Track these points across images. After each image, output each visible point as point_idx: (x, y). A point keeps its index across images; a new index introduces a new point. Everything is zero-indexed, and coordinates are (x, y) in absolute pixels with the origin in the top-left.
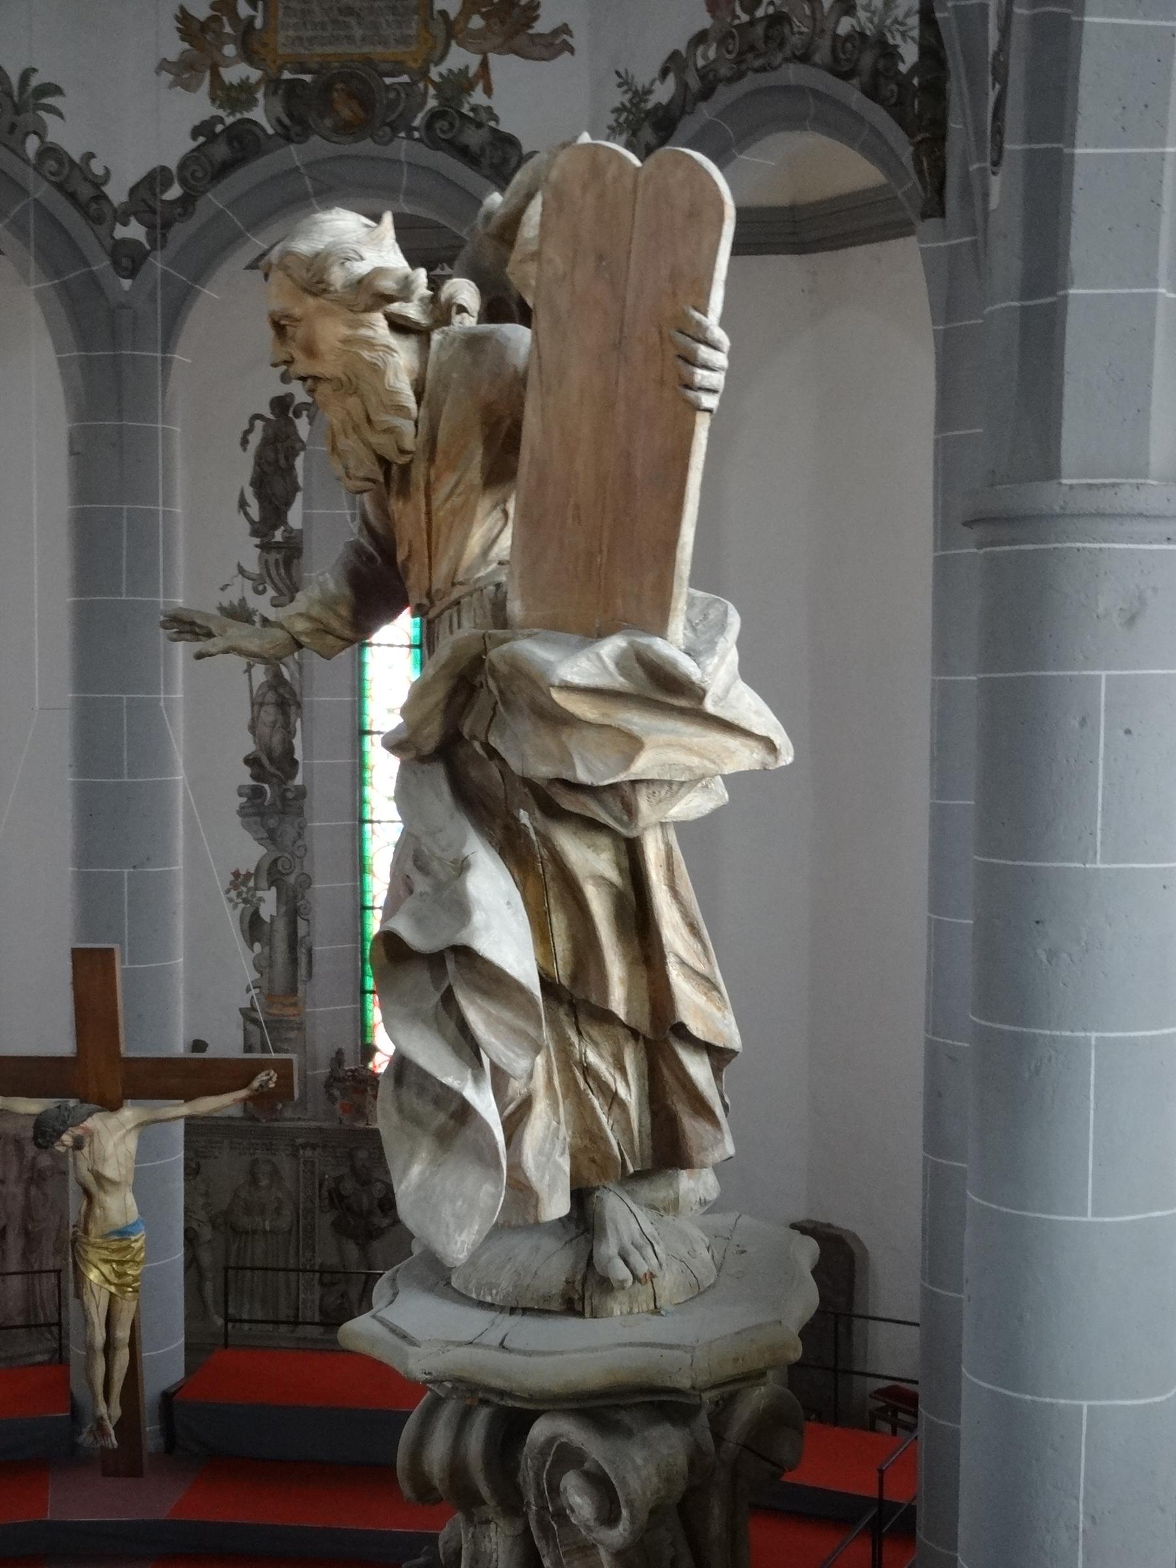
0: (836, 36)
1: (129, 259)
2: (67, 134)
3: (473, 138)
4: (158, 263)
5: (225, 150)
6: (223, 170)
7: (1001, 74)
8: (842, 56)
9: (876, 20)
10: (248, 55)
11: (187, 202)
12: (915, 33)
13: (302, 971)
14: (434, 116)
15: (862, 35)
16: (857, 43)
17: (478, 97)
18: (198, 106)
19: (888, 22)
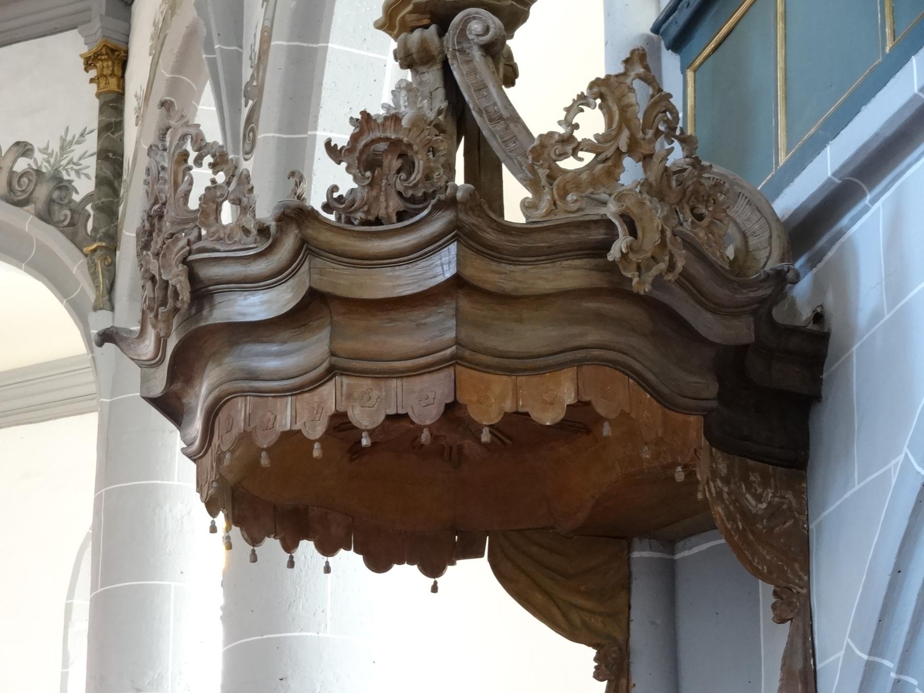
0: (12, 173)
7: (255, 92)
8: (17, 187)
9: (52, 160)
12: (92, 172)
15: (38, 172)
16: (34, 178)
19: (64, 162)
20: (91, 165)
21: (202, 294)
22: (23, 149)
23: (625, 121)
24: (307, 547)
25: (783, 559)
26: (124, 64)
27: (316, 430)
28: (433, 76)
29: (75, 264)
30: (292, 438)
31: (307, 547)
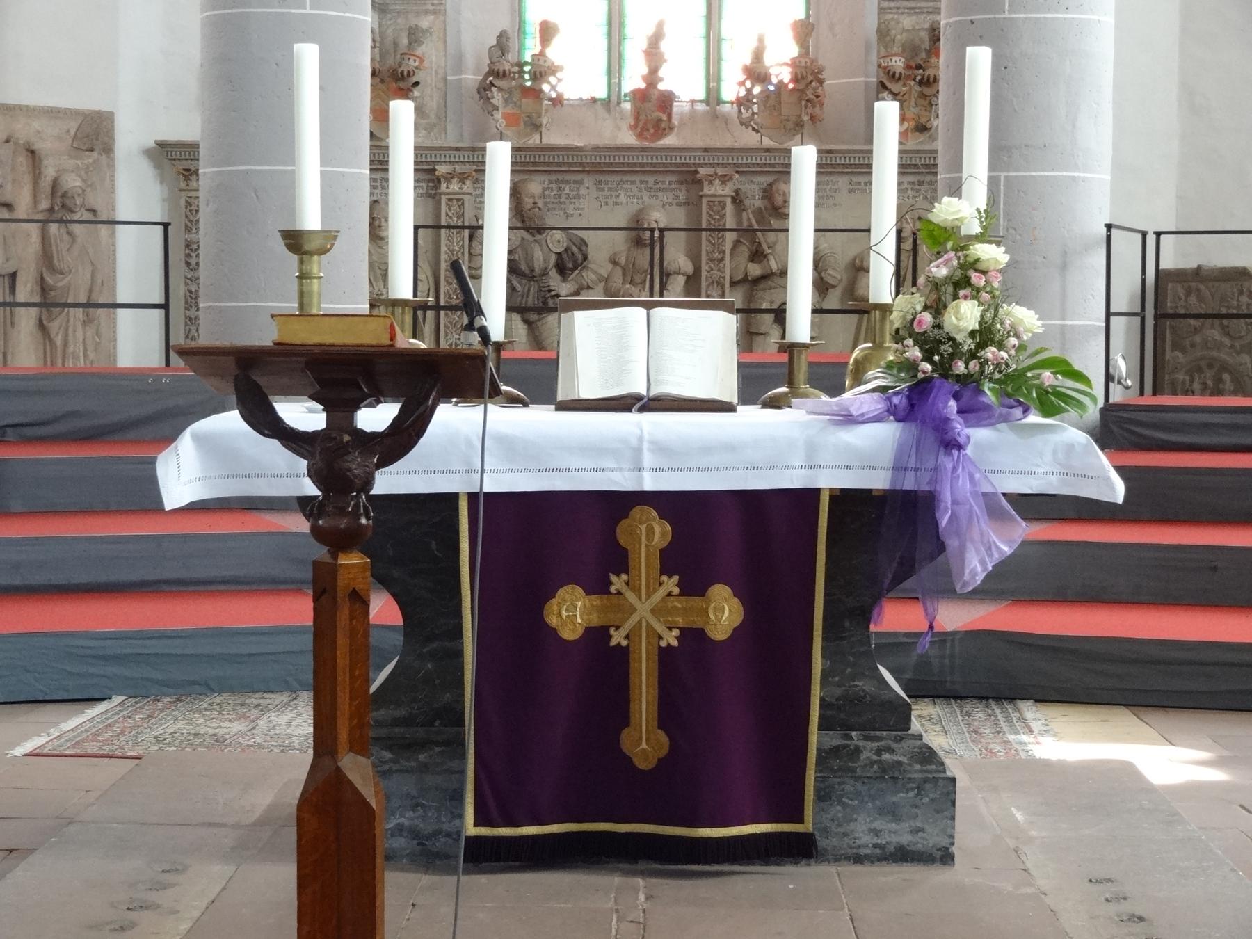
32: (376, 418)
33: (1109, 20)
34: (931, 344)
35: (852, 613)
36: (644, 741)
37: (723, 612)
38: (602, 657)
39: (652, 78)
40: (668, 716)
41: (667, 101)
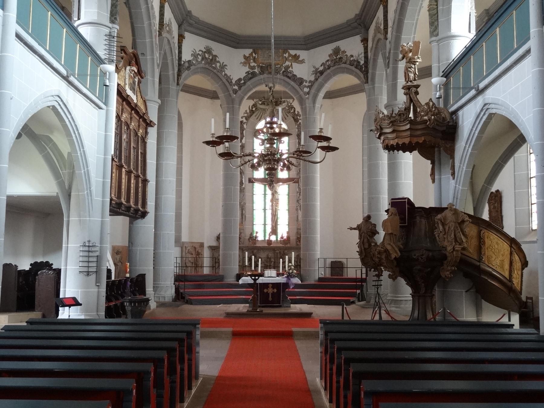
1: (235, 92)
2: (228, 72)
3: (290, 75)
4: (239, 92)
5: (251, 76)
6: (251, 78)
7: (389, 58)
10: (254, 62)
11: (245, 83)
13: (244, 219)
14: (283, 72)
17: (290, 69)
18: (247, 69)
20: (363, 58)
21: (381, 129)
22: (352, 56)
23: (429, 108)
24: (396, 151)
25: (451, 153)
26: (367, 41)
27: (395, 144)
28: (408, 96)
29: (362, 75)
30: (392, 145)
31: (396, 151)
32: (257, 278)
33: (319, 236)
34: (289, 273)
35: (284, 291)
36: (270, 299)
37: (275, 290)
38: (267, 294)
39: (269, 238)
40: (272, 297)
41: (271, 241)
